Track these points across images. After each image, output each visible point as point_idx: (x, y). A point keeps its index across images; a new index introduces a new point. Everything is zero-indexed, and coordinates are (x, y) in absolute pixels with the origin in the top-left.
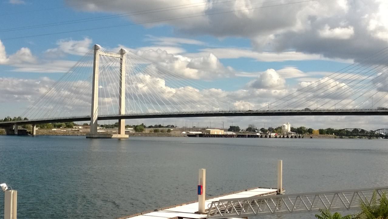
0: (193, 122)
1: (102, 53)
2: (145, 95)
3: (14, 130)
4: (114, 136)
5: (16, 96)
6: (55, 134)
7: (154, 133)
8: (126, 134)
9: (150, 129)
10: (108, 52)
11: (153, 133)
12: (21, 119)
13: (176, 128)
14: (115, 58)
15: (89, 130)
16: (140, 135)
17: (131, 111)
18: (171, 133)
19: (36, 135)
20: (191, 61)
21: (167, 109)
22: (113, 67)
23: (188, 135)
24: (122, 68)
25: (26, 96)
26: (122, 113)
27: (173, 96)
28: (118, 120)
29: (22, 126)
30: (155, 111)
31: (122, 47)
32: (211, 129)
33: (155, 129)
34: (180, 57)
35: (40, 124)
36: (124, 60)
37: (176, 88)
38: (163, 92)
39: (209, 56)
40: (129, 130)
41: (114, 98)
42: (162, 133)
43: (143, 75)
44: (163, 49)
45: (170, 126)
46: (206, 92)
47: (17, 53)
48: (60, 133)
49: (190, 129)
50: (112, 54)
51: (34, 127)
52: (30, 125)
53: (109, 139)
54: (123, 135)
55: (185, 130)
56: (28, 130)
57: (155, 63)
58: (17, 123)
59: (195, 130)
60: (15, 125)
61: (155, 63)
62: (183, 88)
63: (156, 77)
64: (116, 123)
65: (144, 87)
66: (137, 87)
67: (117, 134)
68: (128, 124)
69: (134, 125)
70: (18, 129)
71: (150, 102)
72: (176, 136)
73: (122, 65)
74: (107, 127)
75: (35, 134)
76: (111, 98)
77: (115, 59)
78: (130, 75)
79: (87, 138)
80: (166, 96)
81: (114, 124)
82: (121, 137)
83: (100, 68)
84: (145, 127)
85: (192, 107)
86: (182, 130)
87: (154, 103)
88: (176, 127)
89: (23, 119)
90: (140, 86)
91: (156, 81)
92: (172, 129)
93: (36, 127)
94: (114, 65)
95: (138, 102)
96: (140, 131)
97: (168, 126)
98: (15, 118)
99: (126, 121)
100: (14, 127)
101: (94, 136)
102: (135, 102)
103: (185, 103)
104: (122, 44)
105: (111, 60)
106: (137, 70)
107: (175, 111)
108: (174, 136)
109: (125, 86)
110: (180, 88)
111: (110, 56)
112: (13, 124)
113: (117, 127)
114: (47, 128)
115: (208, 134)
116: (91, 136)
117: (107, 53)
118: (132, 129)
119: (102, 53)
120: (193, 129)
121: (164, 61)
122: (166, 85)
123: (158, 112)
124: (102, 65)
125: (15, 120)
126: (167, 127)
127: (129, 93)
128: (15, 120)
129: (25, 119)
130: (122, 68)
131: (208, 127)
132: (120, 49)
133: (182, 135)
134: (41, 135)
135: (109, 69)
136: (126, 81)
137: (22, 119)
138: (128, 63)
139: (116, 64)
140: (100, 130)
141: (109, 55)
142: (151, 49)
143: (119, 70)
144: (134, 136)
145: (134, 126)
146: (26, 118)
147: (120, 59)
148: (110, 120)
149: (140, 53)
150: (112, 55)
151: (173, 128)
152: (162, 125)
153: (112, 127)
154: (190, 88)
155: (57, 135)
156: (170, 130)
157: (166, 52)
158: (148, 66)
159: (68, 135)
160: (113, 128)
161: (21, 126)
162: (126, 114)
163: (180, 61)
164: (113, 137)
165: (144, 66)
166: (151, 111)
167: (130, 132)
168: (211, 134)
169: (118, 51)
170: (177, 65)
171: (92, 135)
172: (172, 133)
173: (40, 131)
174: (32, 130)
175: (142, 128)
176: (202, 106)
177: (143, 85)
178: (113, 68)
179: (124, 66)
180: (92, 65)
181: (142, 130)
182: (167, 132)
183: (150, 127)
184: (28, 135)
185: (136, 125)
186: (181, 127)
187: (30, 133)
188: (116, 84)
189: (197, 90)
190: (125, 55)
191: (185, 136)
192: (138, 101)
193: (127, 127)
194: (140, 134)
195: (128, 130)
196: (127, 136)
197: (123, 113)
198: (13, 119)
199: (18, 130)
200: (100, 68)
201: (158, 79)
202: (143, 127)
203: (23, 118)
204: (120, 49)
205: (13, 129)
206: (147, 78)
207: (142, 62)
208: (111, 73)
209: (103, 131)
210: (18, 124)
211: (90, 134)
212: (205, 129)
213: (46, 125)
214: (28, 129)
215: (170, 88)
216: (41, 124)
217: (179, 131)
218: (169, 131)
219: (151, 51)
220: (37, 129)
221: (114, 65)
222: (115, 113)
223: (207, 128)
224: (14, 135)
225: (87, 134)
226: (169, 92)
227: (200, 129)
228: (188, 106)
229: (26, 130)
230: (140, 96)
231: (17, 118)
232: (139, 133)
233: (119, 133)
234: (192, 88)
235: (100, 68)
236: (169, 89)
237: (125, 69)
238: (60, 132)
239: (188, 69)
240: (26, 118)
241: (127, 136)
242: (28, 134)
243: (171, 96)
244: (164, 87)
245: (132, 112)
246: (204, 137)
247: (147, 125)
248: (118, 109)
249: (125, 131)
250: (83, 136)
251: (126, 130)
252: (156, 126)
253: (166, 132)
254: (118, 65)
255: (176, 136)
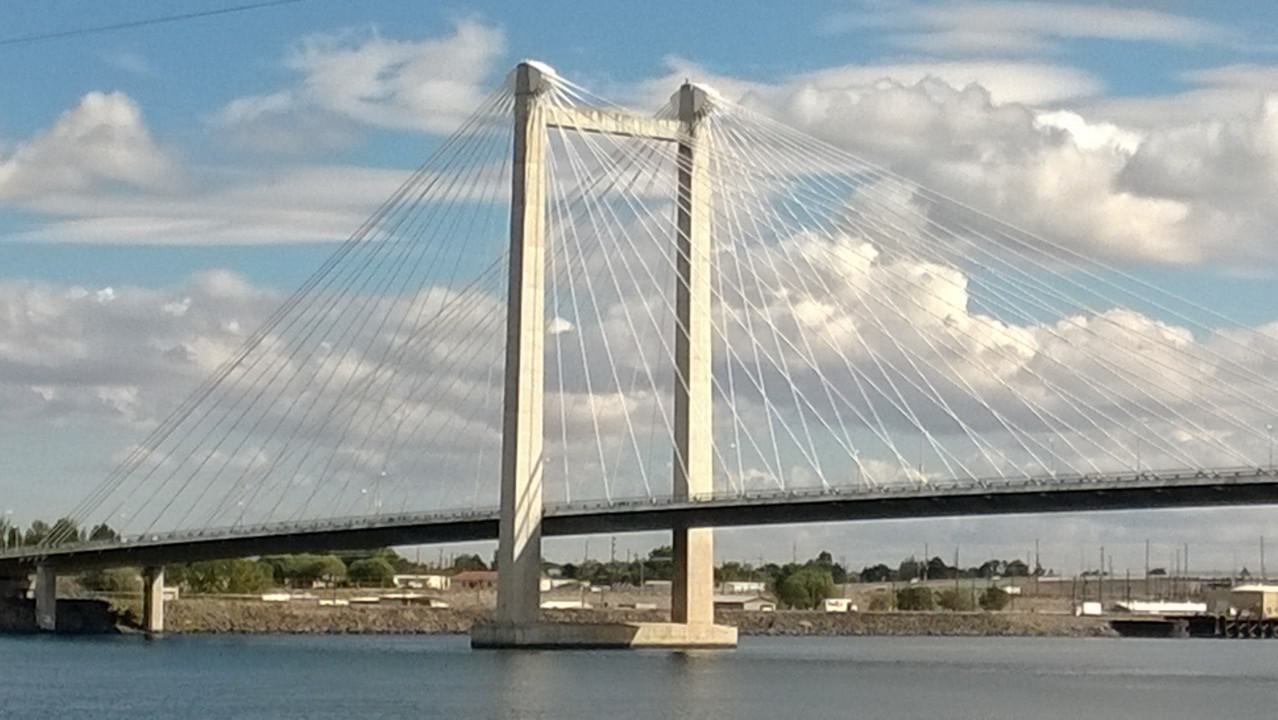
0: (1148, 542)
1: (563, 116)
2: (835, 370)
3: (33, 601)
4: (648, 634)
5: (49, 393)
6: (283, 627)
7: (896, 611)
8: (719, 618)
9: (874, 586)
10: (604, 104)
11: (890, 610)
12: (74, 536)
13: (1041, 579)
14: (645, 142)
15: (489, 598)
16: (807, 624)
17: (754, 473)
18: (1005, 611)
19: (165, 630)
20: (1142, 146)
21: (982, 456)
22: (633, 200)
23: (1116, 625)
24: (689, 207)
25: (104, 393)
26: (692, 492)
27: (1023, 376)
28: (669, 533)
29: (84, 575)
30: (900, 473)
31: (688, 73)
32: (1266, 582)
33: (901, 586)
34: (1065, 120)
35: (189, 565)
36: (701, 157)
37: (1032, 324)
38: (955, 351)
39: (1260, 111)
40: (741, 593)
41: (642, 393)
42: (949, 612)
43: (824, 244)
44: (958, 77)
45: (1001, 570)
46: (1238, 344)
47: (62, 130)
48: (310, 620)
49: (1129, 589)
50: (626, 117)
51: (152, 581)
52: (129, 569)
53: (620, 652)
54: (702, 627)
55: (1094, 593)
56: (118, 605)
57: (905, 167)
58: (50, 556)
59: (1163, 591)
60: (39, 569)
61: (905, 167)
62: (1081, 321)
63: (921, 255)
64: (656, 553)
65: (829, 319)
66: (789, 326)
67: (662, 620)
68: (734, 560)
69: (773, 566)
70: (59, 596)
71: (874, 422)
72: (1041, 634)
73: (689, 186)
74: (602, 575)
75: (157, 624)
76: (627, 395)
77: (645, 147)
78: (739, 247)
79: (476, 645)
80: (974, 377)
81: (645, 555)
82: (688, 641)
83: (555, 209)
84: (839, 573)
85: (1137, 444)
86: (1082, 588)
87: (897, 422)
88: (1039, 571)
89: (88, 537)
90: (810, 311)
91: (910, 286)
92: (1013, 585)
93: (167, 583)
94: (642, 190)
95: (793, 420)
96: (807, 600)
97: (987, 565)
98: (39, 525)
99: (714, 532)
100: (34, 584)
101: (519, 637)
102: (775, 419)
103: (1099, 418)
104: (689, 57)
105: (619, 156)
106: (784, 213)
107: (1031, 469)
108: (1025, 634)
109: (713, 317)
110: (1065, 325)
111: (617, 133)
112: (29, 565)
113: (662, 577)
114: (233, 588)
115: (1245, 614)
116: (504, 636)
117: (595, 115)
118: (761, 586)
119: (563, 116)
120: (1146, 582)
121: (967, 153)
122: (972, 308)
123: (925, 480)
124: (562, 189)
125: (40, 537)
126: (983, 572)
127: (734, 361)
128: (40, 537)
129: (102, 532)
130: (693, 202)
131: (1245, 572)
132: (678, 88)
133: (1080, 627)
134: (196, 631)
135: (608, 213)
136: (714, 282)
137: (83, 534)
138: (725, 171)
139: (651, 183)
140: (557, 598)
141: (609, 124)
142: (888, 79)
143: (670, 216)
144: (771, 631)
145: (771, 568)
146: (104, 527)
147: (675, 146)
148: (620, 535)
149: (811, 102)
150: (628, 123)
151: (1023, 580)
152: (948, 563)
153: (634, 575)
154: (1132, 323)
155: (293, 633)
156: (1003, 593)
157: (986, 94)
158: (861, 191)
159: (361, 627)
160: (636, 582)
161: (74, 578)
162: (721, 497)
163: (1067, 152)
164: (638, 639)
165: (845, 187)
166: (876, 475)
167: (747, 607)
168: (1268, 615)
169: (667, 101)
170: (1050, 178)
171: (513, 626)
172: (1011, 613)
173: (188, 608)
174: (142, 603)
175: (821, 580)
176: (1212, 433)
177: (829, 310)
178: (637, 206)
179: (700, 189)
180: (507, 190)
181: (819, 594)
182: (983, 602)
183: (872, 574)
184: (119, 632)
185: (781, 564)
186: (1069, 571)
187: (127, 618)
188: (656, 305)
189: (1179, 336)
190: (706, 120)
191: (1097, 633)
192: (797, 410)
193: (725, 574)
194: (808, 617)
195: (732, 593)
196: (729, 634)
197: (702, 486)
198: (29, 532)
199: (60, 602)
200: (555, 209)
201: (927, 267)
202: (829, 574)
203: (86, 526)
204: (675, 85)
205: (30, 595)
206: (854, 259)
207: (821, 166)
208: (620, 237)
209: (577, 604)
210: (61, 563)
211: (494, 625)
212: (1226, 584)
213: (228, 572)
214: (117, 597)
215: (997, 324)
216: (194, 564)
217: (1058, 597)
218: (994, 598)
219: (883, 86)
220: (169, 597)
221: (639, 188)
222: (649, 488)
223: (1245, 576)
224: (31, 630)
225: (481, 626)
226: (995, 354)
227: (1193, 586)
228: (1114, 437)
229: (104, 599)
230: (807, 379)
231: (51, 525)
232: (804, 612)
233: (679, 615)
234: (1146, 322)
235: (553, 211)
236: (992, 333)
237: (706, 210)
238: (311, 613)
239: (1124, 197)
240: (104, 527)
241: (729, 634)
242: (120, 627)
243: (1011, 378)
244: (964, 322)
245: (761, 479)
246: (1223, 635)
247: (855, 565)
248: (671, 465)
249: (717, 605)
250: (455, 633)
251: (722, 593)
252: (909, 570)
253: (973, 608)
254: (666, 183)
255: (1042, 628)
